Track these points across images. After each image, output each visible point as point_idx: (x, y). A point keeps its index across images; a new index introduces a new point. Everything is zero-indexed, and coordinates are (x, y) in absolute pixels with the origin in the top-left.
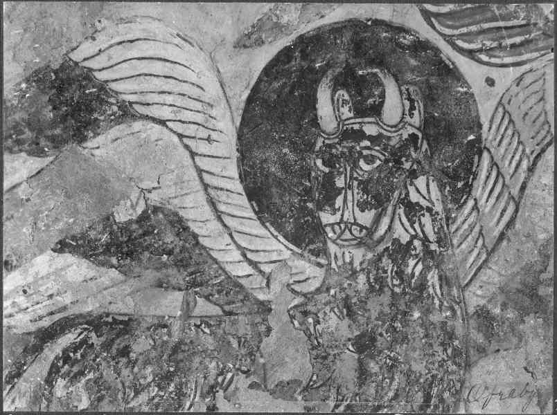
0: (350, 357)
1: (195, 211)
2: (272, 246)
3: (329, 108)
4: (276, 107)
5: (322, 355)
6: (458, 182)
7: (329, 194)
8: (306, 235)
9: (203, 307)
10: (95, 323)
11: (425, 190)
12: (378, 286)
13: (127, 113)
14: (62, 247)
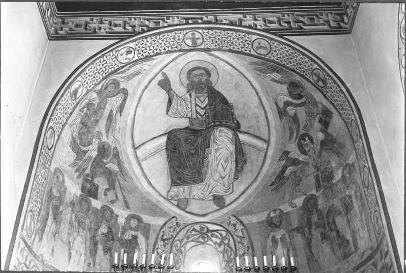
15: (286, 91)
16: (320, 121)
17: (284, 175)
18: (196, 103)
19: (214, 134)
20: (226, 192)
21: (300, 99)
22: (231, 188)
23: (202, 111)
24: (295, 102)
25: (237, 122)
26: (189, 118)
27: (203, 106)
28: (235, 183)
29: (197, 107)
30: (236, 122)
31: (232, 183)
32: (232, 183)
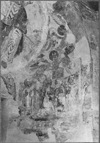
0: (54, 65)
1: (47, 60)
2: (51, 61)
3: (53, 54)
4: (50, 55)
5: (53, 65)
6: (58, 56)
7: (53, 58)
8: (52, 60)
9: (48, 64)
10: (43, 65)
11: (57, 57)
12: (55, 61)
13: (44, 56)
14: (42, 62)
15: (57, 28)
16: (66, 49)
17: (38, 65)
18: (11, 10)
19: (13, 30)
20: (8, 62)
21: (62, 35)
22: (11, 61)
23: (12, 16)
24: (59, 35)
25: (26, 31)
26: (5, 16)
27: (14, 14)
28: (14, 59)
29: (11, 12)
30: (25, 30)
31: (13, 58)
32: (13, 58)
